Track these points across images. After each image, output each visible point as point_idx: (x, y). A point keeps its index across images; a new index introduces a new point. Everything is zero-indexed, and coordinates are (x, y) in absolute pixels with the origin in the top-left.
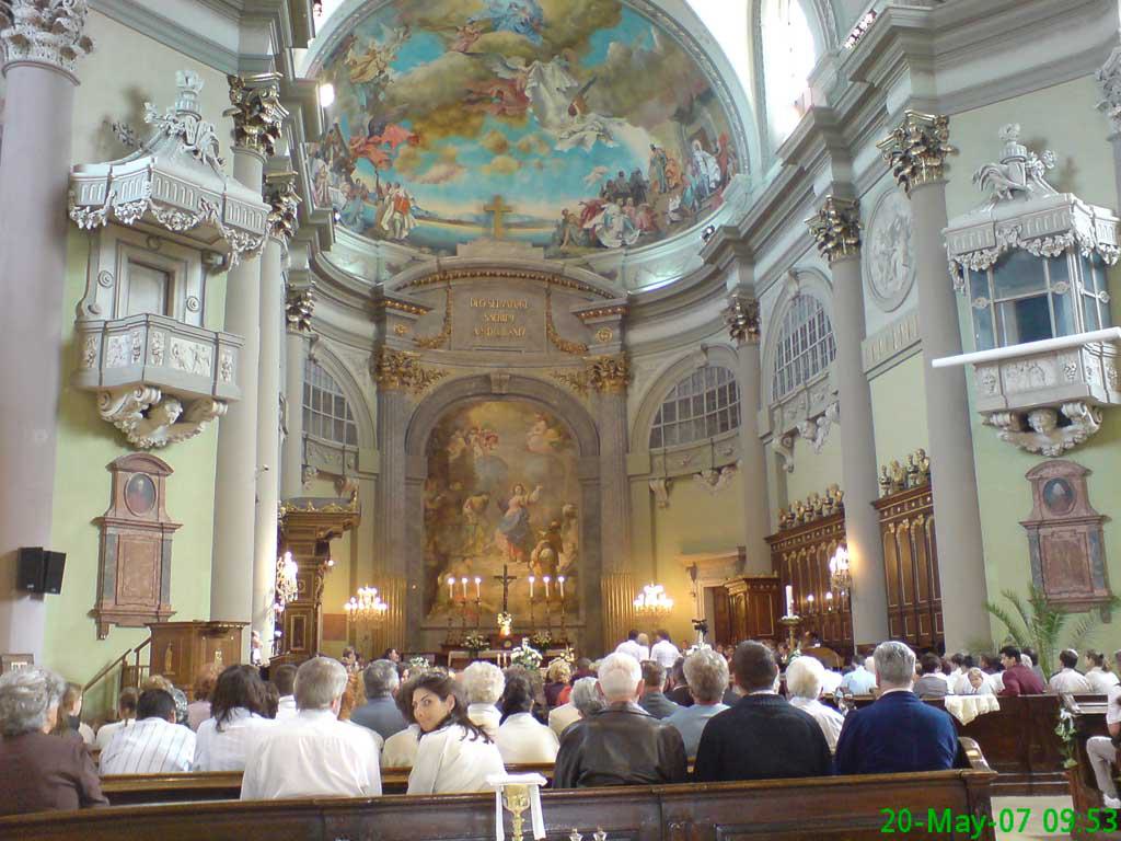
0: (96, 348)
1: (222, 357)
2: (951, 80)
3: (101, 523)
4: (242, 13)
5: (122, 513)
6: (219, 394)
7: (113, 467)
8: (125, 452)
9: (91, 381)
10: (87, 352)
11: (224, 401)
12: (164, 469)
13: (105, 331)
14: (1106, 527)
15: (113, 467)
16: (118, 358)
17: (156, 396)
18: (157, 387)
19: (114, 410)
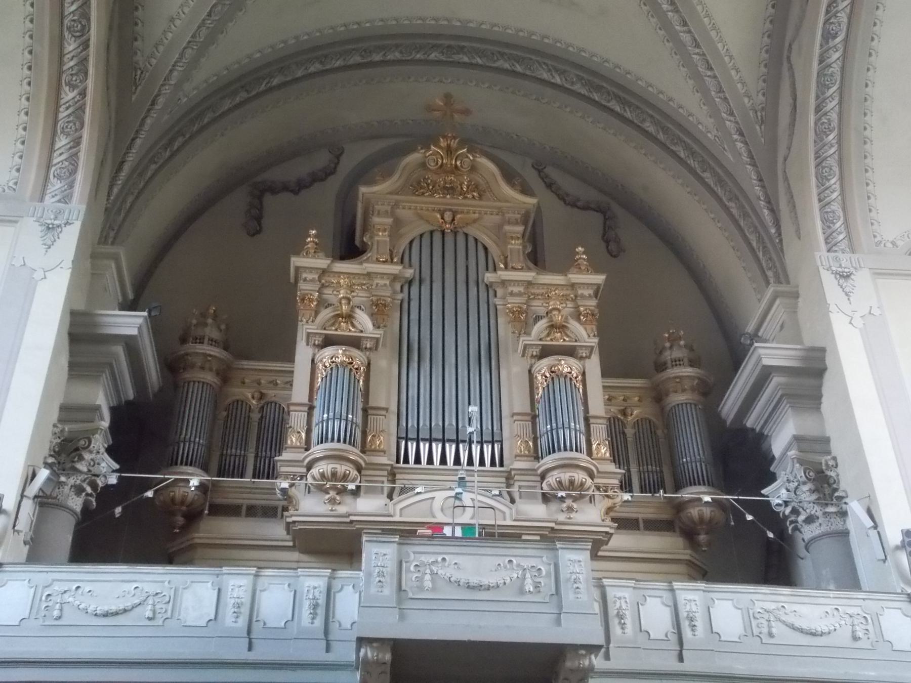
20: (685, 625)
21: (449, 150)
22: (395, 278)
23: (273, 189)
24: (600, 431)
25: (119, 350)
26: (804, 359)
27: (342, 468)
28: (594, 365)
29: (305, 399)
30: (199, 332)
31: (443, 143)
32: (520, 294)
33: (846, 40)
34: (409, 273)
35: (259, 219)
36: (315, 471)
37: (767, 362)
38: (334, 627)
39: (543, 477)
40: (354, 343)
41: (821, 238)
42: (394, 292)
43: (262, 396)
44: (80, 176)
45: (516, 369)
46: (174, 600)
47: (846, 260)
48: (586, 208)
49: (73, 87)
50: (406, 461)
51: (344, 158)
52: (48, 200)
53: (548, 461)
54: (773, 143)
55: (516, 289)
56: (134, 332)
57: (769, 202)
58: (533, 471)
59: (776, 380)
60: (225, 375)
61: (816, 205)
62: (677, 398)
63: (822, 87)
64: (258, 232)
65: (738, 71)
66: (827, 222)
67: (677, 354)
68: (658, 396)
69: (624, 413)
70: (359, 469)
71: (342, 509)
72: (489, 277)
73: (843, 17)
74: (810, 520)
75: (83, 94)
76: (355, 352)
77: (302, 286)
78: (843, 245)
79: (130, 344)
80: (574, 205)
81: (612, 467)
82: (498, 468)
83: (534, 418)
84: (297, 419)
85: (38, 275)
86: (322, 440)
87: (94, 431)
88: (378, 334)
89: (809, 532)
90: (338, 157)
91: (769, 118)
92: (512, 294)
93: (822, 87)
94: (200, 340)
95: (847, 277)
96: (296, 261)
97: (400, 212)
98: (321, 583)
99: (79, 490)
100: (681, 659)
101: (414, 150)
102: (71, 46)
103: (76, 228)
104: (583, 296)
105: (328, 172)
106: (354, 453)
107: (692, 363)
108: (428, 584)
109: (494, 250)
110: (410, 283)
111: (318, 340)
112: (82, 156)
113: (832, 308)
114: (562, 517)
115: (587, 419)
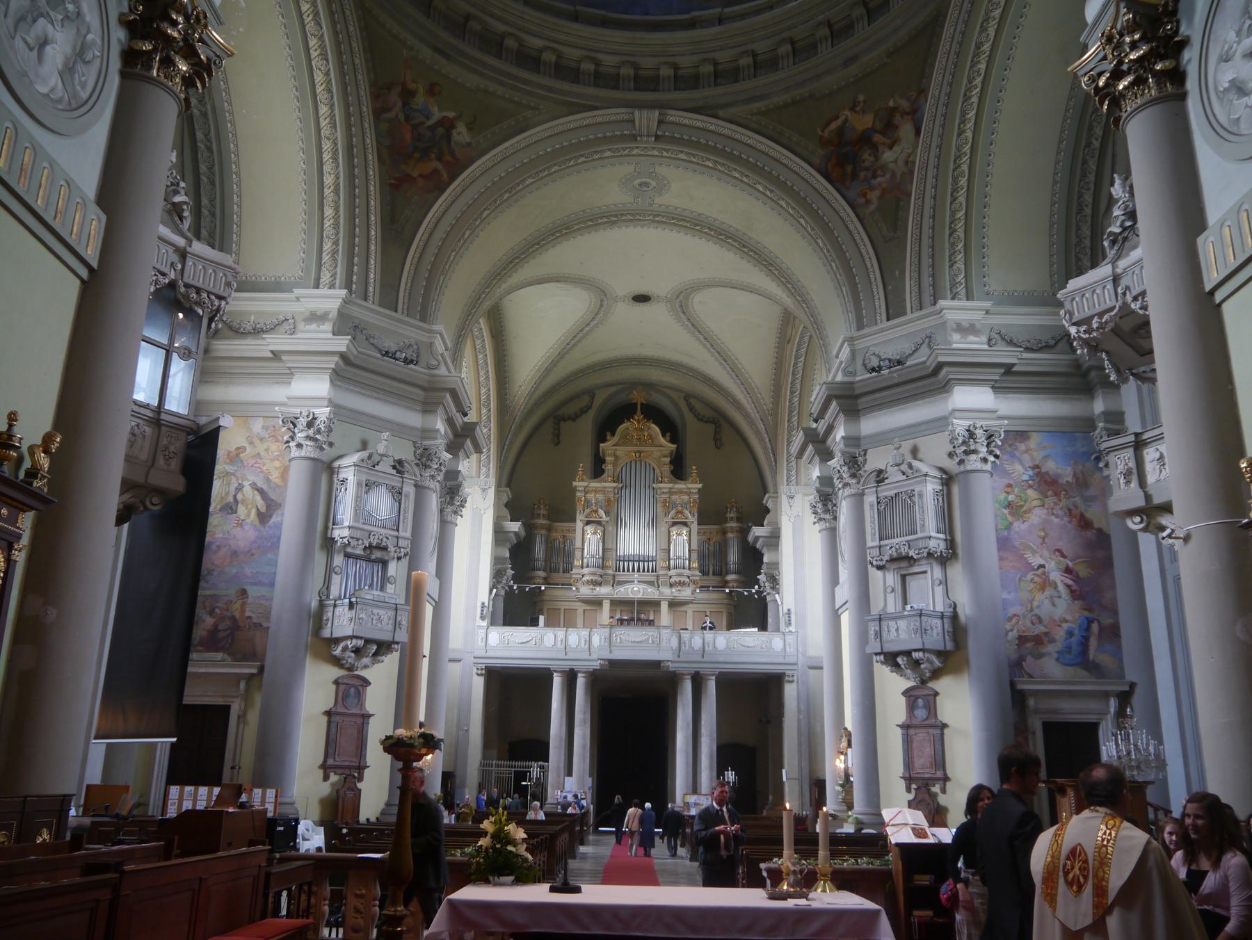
0: (330, 614)
1: (399, 619)
2: (869, 425)
3: (328, 713)
4: (423, 403)
5: (341, 709)
6: (396, 639)
7: (336, 682)
8: (343, 672)
9: (326, 633)
10: (325, 618)
11: (398, 643)
12: (366, 682)
13: (335, 606)
14: (946, 731)
15: (336, 682)
16: (342, 623)
17: (360, 643)
18: (361, 638)
19: (338, 651)
20: (706, 645)
21: (638, 422)
22: (615, 488)
23: (564, 419)
24: (695, 556)
25: (512, 535)
26: (771, 532)
27: (594, 578)
28: (695, 527)
29: (581, 546)
30: (538, 512)
31: (636, 418)
32: (666, 493)
33: (800, 394)
34: (620, 485)
35: (558, 436)
36: (585, 578)
37: (757, 534)
38: (592, 647)
39: (671, 577)
40: (599, 523)
41: (785, 478)
42: (615, 494)
43: (564, 536)
44: (491, 465)
45: (663, 529)
46: (542, 639)
47: (793, 489)
48: (707, 422)
49: (486, 427)
50: (619, 571)
51: (595, 399)
52: (482, 477)
53: (672, 572)
54: (776, 425)
55: (665, 491)
56: (517, 530)
57: (773, 451)
58: (666, 575)
59: (761, 540)
60: (549, 529)
61: (785, 463)
62: (730, 535)
63: (791, 412)
64: (558, 443)
65: (761, 394)
66: (789, 471)
67: (732, 515)
68: (724, 532)
69: (709, 539)
70: (601, 576)
71: (595, 592)
72: (655, 486)
73: (798, 386)
74: (768, 594)
75: (490, 430)
76: (600, 527)
77: (578, 494)
78: (793, 482)
79: (515, 533)
80: (701, 420)
81: (697, 573)
82: (654, 573)
83: (669, 550)
84: (578, 554)
85: (482, 512)
86: (588, 566)
87: (507, 569)
88: (608, 519)
89: (768, 598)
90: (593, 398)
91: (775, 412)
92: (663, 493)
93: (791, 412)
94: (539, 516)
95: (792, 498)
96: (574, 484)
97: (618, 453)
98: (588, 633)
99: (503, 588)
100: (703, 657)
101: (623, 422)
102: (484, 411)
103: (493, 488)
104: (693, 493)
105: (588, 408)
106: (600, 571)
107: (739, 520)
108: (619, 641)
109: (657, 471)
110: (622, 487)
111: (585, 522)
112: (491, 455)
113: (783, 513)
114: (676, 594)
115: (689, 551)
